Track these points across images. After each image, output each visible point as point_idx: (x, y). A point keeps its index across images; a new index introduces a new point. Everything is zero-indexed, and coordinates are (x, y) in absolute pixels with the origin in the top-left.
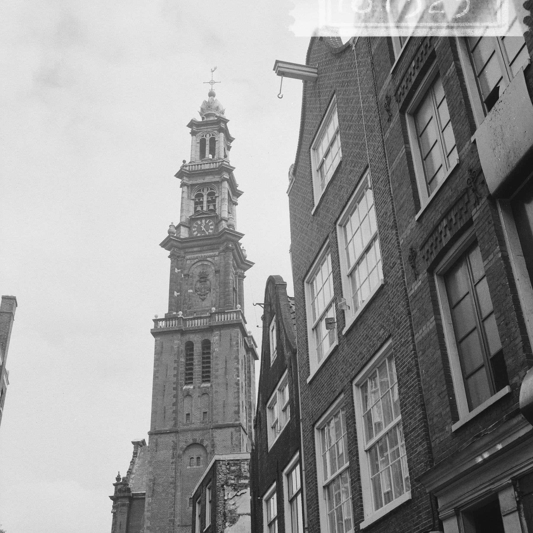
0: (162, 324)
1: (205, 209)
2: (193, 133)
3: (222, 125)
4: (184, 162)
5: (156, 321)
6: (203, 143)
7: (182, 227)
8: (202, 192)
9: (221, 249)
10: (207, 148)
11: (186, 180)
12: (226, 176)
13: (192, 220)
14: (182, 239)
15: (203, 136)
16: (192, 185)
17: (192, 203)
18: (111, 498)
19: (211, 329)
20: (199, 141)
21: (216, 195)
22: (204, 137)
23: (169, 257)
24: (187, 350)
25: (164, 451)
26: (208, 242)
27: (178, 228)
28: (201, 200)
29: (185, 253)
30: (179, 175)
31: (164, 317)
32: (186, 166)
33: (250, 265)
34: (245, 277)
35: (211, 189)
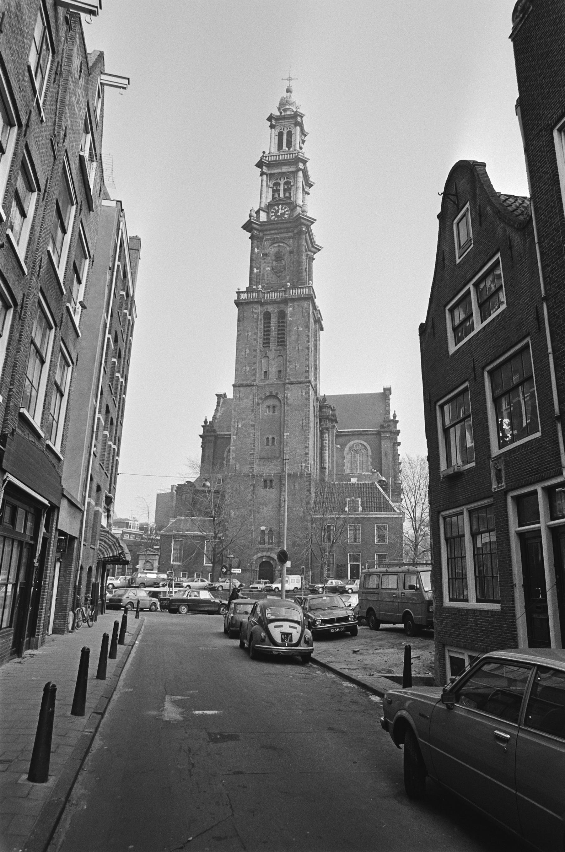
0: (243, 296)
1: (282, 196)
2: (272, 127)
3: (299, 119)
4: (264, 152)
5: (239, 293)
6: (280, 135)
8: (279, 181)
9: (296, 231)
11: (265, 169)
12: (301, 166)
13: (270, 206)
14: (261, 222)
16: (271, 174)
18: (200, 436)
19: (285, 301)
21: (292, 184)
23: (250, 238)
24: (265, 319)
26: (285, 225)
27: (258, 212)
28: (278, 188)
30: (260, 165)
31: (245, 290)
32: (266, 157)
34: (314, 259)
35: (287, 178)
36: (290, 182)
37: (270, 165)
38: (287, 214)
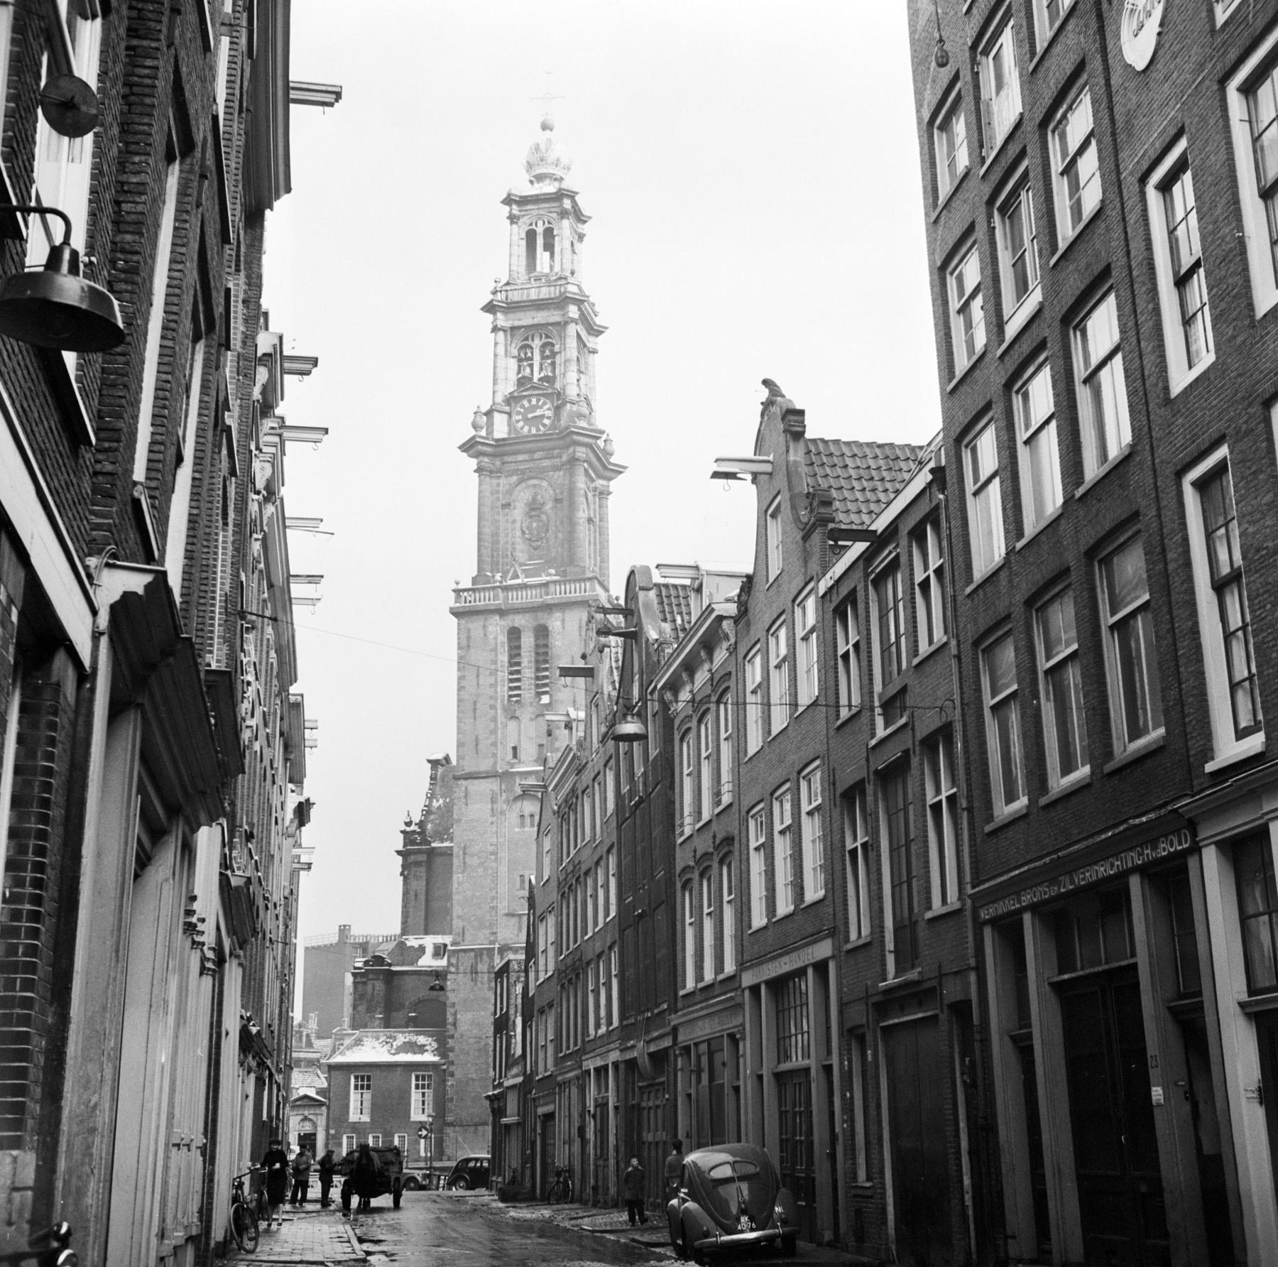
2: (513, 219)
6: (531, 235)
7: (496, 414)
8: (530, 342)
9: (565, 458)
10: (540, 241)
11: (502, 320)
12: (573, 311)
13: (511, 400)
16: (513, 328)
17: (513, 364)
18: (399, 853)
19: (549, 608)
20: (523, 235)
21: (557, 348)
24: (509, 640)
25: (478, 806)
30: (490, 308)
33: (618, 471)
36: (553, 345)
37: (512, 307)
38: (549, 418)
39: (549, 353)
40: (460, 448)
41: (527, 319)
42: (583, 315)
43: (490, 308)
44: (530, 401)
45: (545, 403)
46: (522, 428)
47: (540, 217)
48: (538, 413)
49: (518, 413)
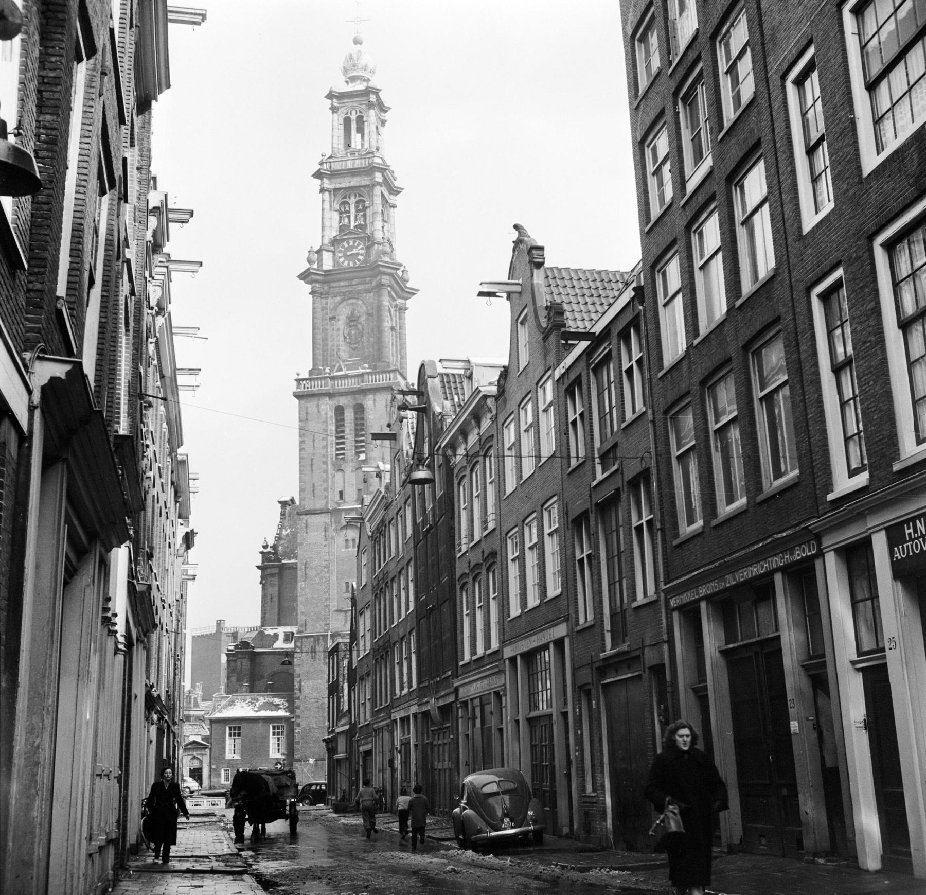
2: (334, 109)
6: (347, 121)
7: (324, 252)
8: (348, 200)
9: (374, 284)
10: (354, 126)
11: (327, 184)
12: (378, 177)
13: (335, 242)
15: (347, 113)
16: (335, 190)
17: (336, 216)
18: (259, 567)
19: (364, 392)
20: (342, 121)
21: (367, 204)
22: (349, 115)
23: (310, 294)
25: (315, 534)
29: (330, 288)
30: (318, 175)
33: (412, 293)
36: (364, 202)
37: (334, 174)
38: (362, 255)
39: (362, 208)
40: (299, 277)
41: (345, 183)
42: (385, 179)
43: (318, 175)
44: (348, 243)
45: (359, 245)
46: (343, 262)
47: (353, 108)
48: (355, 251)
49: (340, 252)
